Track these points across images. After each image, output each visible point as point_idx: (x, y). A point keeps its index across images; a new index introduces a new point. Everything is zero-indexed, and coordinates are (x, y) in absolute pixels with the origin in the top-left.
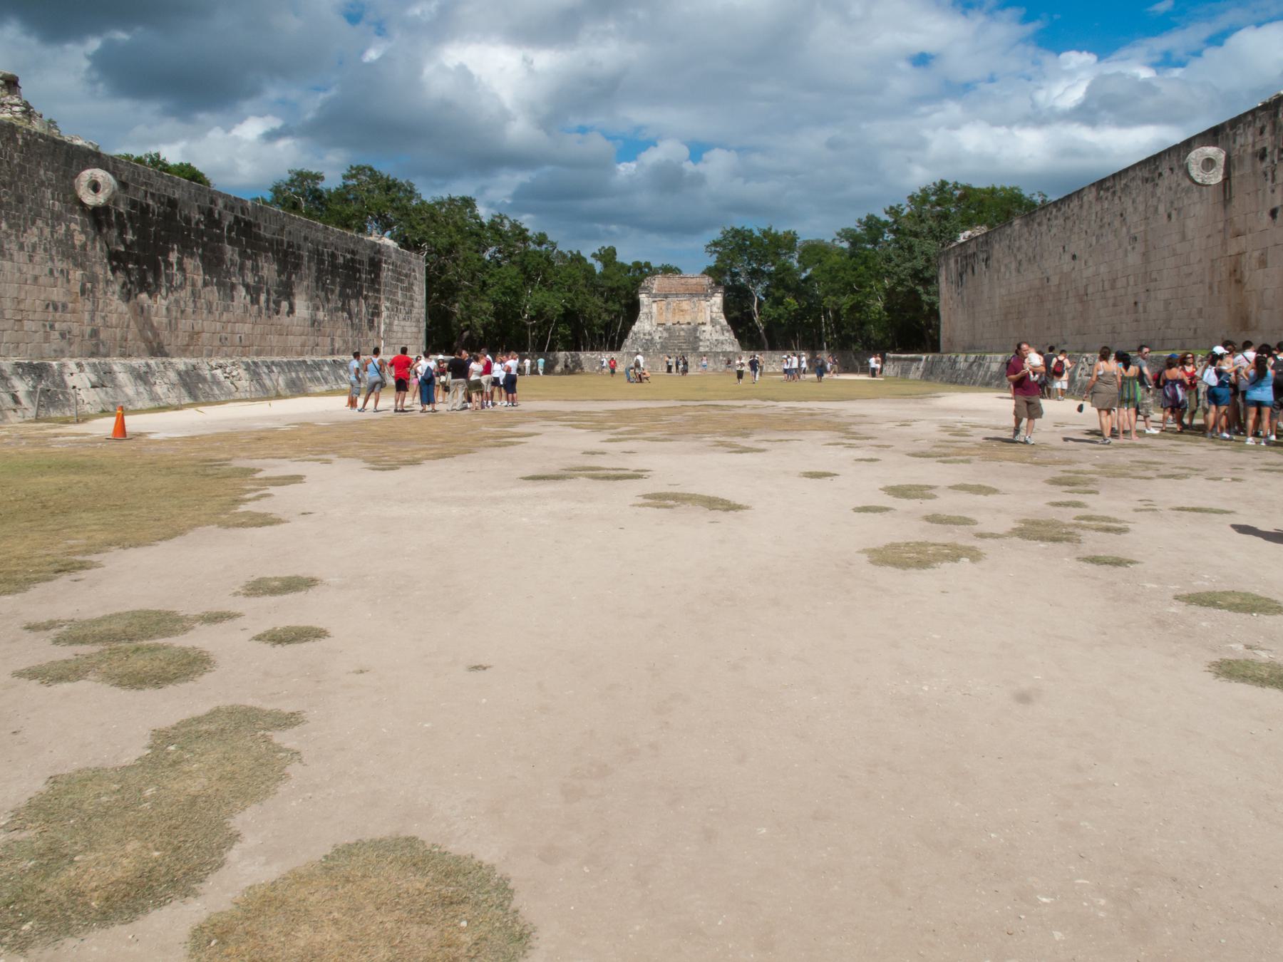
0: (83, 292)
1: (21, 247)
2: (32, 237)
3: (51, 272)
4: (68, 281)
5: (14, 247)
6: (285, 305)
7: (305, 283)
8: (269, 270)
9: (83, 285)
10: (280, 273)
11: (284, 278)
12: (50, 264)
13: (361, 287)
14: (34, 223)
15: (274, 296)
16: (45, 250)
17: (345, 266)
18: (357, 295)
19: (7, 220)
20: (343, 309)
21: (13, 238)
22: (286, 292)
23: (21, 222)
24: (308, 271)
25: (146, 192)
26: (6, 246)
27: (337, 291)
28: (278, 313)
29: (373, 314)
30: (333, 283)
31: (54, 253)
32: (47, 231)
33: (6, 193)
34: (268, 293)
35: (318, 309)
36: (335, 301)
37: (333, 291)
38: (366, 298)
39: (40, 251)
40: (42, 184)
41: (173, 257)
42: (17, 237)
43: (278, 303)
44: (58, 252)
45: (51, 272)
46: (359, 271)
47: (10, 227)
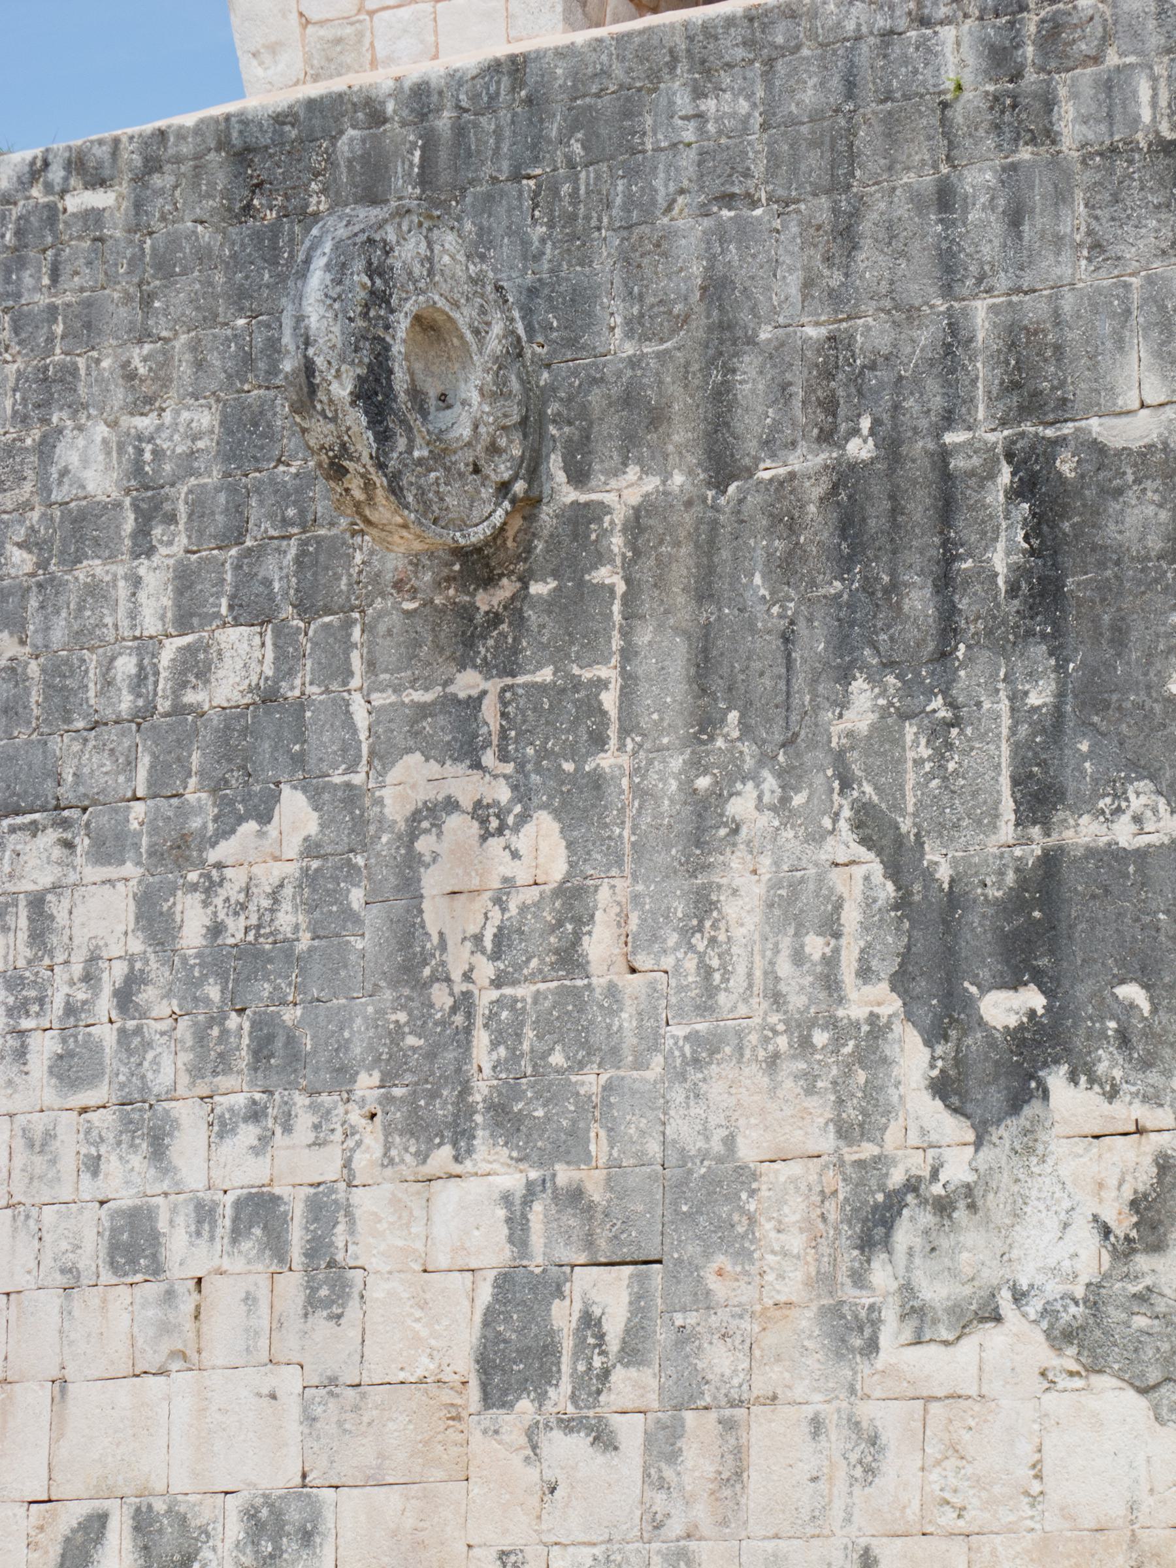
0: (513, 1360)
3: (133, 1246)
4: (330, 1285)
9: (519, 1296)
12: (126, 1178)
16: (71, 1069)
31: (168, 1068)
40: (82, 529)
44: (211, 1060)
45: (133, 1246)
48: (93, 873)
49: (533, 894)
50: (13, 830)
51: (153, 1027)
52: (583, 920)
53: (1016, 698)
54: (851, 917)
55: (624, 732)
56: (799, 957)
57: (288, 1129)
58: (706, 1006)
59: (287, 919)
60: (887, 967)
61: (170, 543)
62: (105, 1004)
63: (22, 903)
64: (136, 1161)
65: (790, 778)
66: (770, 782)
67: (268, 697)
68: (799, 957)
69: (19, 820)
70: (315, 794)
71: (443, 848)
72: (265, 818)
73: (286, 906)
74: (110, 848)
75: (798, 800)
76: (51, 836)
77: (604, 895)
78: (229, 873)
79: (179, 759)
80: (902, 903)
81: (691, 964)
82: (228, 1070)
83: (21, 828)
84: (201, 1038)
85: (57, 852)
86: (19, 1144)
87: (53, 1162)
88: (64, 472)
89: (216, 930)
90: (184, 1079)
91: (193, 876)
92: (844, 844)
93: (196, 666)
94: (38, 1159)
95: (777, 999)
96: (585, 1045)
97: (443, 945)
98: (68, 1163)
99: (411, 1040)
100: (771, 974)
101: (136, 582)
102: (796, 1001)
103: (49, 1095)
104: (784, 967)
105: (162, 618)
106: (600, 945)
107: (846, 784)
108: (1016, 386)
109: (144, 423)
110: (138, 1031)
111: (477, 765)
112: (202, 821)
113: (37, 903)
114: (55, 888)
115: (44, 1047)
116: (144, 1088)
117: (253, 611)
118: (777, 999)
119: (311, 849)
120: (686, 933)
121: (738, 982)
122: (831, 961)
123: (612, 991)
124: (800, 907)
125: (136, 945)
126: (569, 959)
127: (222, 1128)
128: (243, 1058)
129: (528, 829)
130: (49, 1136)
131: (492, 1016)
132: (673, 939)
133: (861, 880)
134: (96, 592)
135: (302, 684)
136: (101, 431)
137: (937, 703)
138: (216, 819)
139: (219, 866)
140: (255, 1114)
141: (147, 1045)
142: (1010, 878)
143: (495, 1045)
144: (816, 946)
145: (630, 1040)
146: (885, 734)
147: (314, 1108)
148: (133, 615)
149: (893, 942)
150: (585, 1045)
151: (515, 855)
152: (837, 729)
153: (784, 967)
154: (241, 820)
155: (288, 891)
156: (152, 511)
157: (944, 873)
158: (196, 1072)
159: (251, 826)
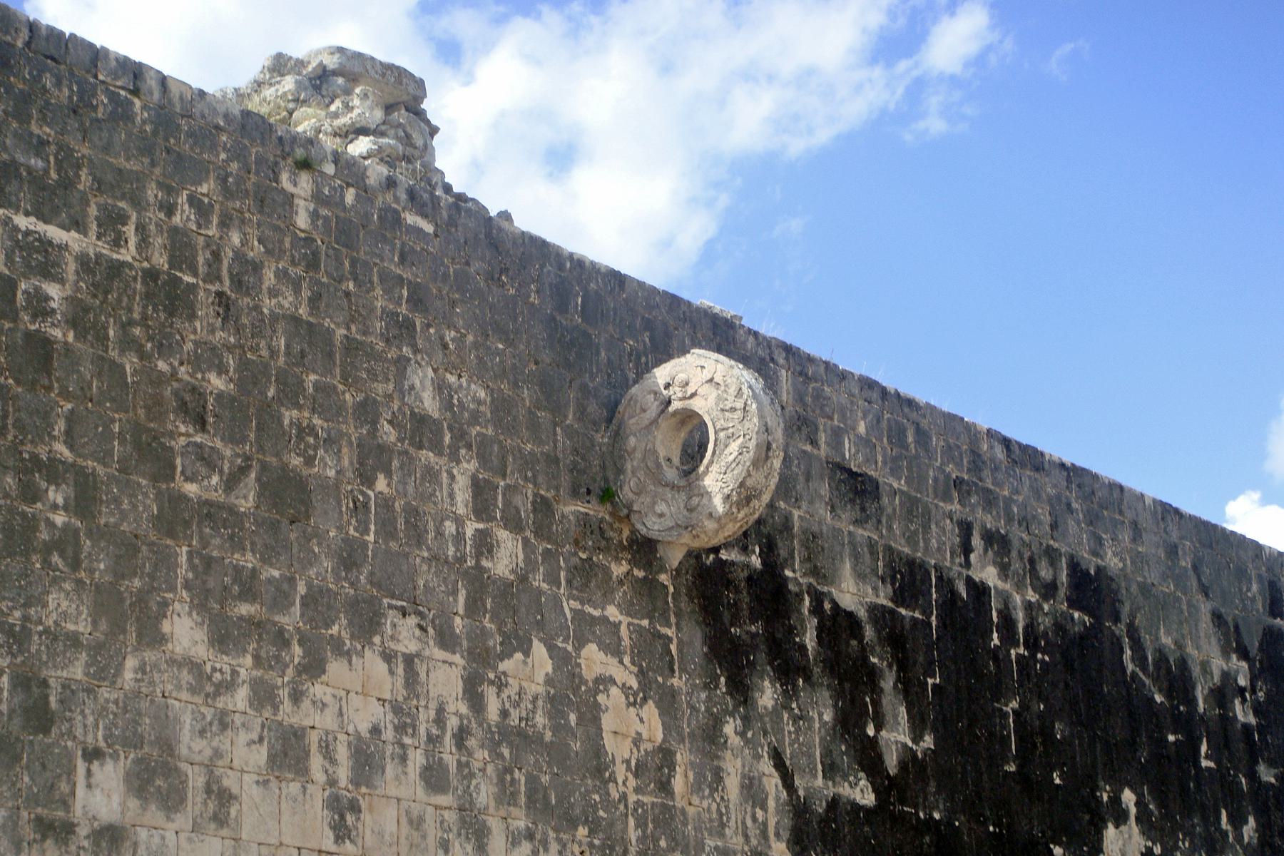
1: (288, 753)
2: (354, 693)
5: (246, 755)
14: (367, 623)
16: (434, 777)
19: (200, 605)
21: (240, 698)
23: (291, 619)
25: (966, 529)
26: (190, 745)
31: (485, 794)
32: (445, 678)
33: (207, 459)
39: (402, 784)
40: (420, 429)
42: (263, 696)
44: (506, 795)
47: (222, 638)
48: (439, 654)
49: (649, 746)
50: (391, 607)
51: (476, 765)
52: (672, 767)
53: (820, 715)
54: (771, 803)
55: (682, 670)
56: (754, 819)
57: (546, 850)
58: (722, 835)
59: (540, 720)
60: (786, 834)
61: (469, 462)
62: (448, 739)
63: (400, 659)
64: (469, 848)
65: (746, 720)
66: (739, 722)
67: (523, 579)
68: (754, 819)
69: (394, 602)
70: (551, 648)
71: (610, 704)
72: (527, 653)
73: (540, 712)
74: (446, 640)
75: (749, 735)
76: (412, 620)
77: (678, 756)
78: (511, 680)
79: (481, 599)
80: (790, 802)
81: (714, 806)
82: (515, 805)
83: (396, 607)
84: (501, 781)
85: (418, 632)
86: (404, 820)
87: (424, 837)
88: (412, 388)
89: (504, 714)
90: (492, 804)
91: (491, 676)
92: (767, 766)
93: (485, 544)
94: (415, 834)
95: (746, 837)
96: (674, 839)
97: (613, 761)
98: (431, 841)
99: (601, 813)
100: (744, 823)
101: (452, 477)
102: (754, 842)
103: (420, 793)
104: (749, 823)
105: (467, 506)
106: (678, 784)
107: (765, 733)
108: (809, 559)
109: (452, 379)
110: (467, 764)
111: (621, 662)
112: (495, 641)
113: (409, 660)
114: (418, 655)
115: (417, 759)
116: (472, 802)
117: (514, 524)
118: (746, 837)
119: (549, 681)
120: (713, 790)
121: (732, 823)
122: (765, 824)
123: (683, 812)
124: (752, 792)
125: (464, 709)
126: (665, 787)
127: (514, 840)
128: (522, 799)
129: (646, 708)
130: (421, 820)
131: (636, 810)
132: (707, 792)
133: (773, 783)
134: (431, 474)
135: (538, 581)
136: (430, 373)
137: (794, 705)
138: (501, 644)
139: (504, 673)
140: (530, 836)
141: (472, 775)
142: (824, 804)
143: (637, 827)
144: (759, 813)
145: (692, 843)
146: (775, 713)
147: (559, 840)
148: (452, 496)
149: (787, 822)
150: (674, 839)
151: (642, 720)
152: (760, 703)
153: (749, 823)
154: (515, 651)
155: (540, 703)
156: (460, 435)
157: (801, 793)
158: (499, 801)
159: (519, 656)
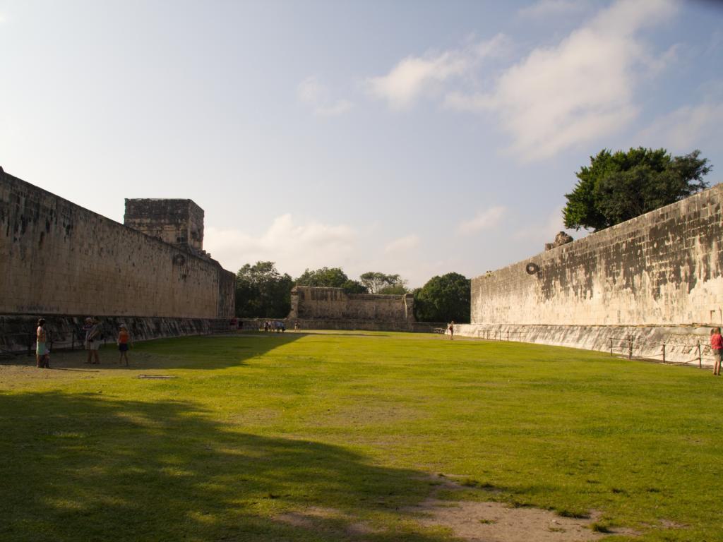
6: (589, 292)
7: (599, 275)
8: (581, 274)
10: (586, 274)
11: (588, 276)
13: (643, 261)
15: (584, 289)
17: (627, 250)
18: (639, 271)
20: (627, 286)
22: (589, 284)
24: (601, 267)
27: (622, 273)
28: (585, 298)
29: (659, 283)
30: (618, 267)
34: (582, 288)
35: (607, 290)
36: (621, 280)
37: (618, 274)
38: (649, 269)
41: (553, 282)
43: (585, 292)
46: (640, 247)
